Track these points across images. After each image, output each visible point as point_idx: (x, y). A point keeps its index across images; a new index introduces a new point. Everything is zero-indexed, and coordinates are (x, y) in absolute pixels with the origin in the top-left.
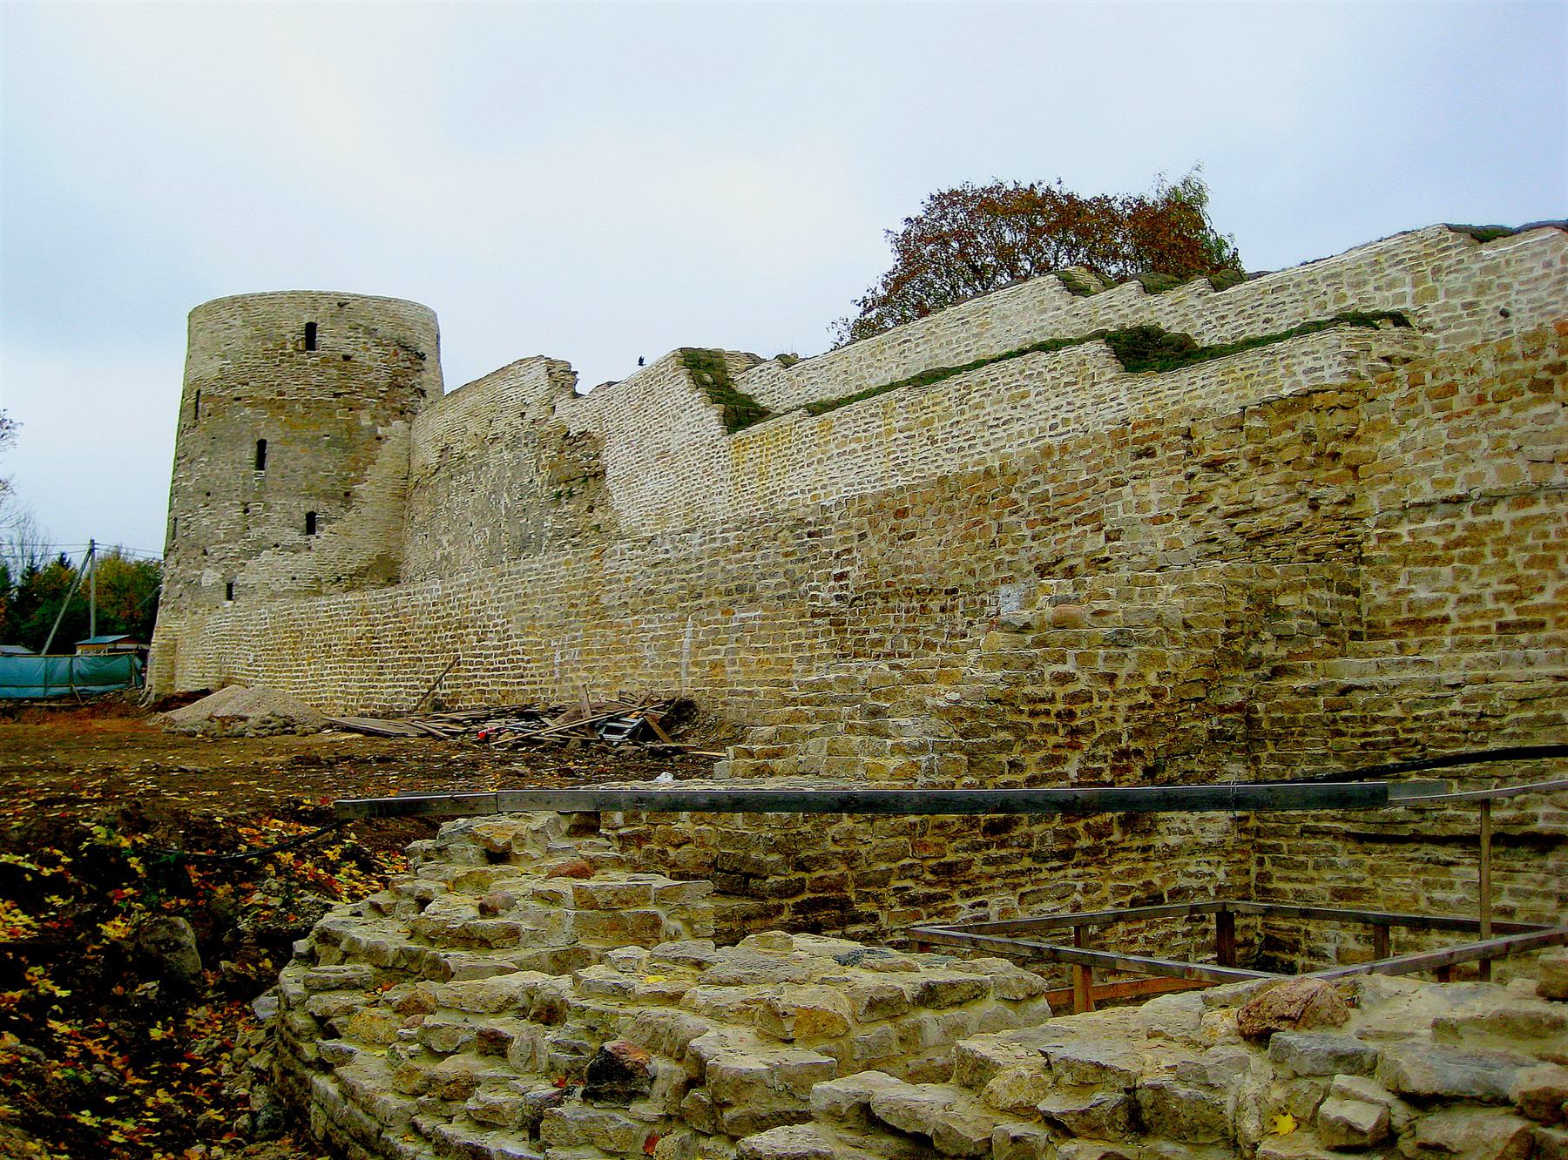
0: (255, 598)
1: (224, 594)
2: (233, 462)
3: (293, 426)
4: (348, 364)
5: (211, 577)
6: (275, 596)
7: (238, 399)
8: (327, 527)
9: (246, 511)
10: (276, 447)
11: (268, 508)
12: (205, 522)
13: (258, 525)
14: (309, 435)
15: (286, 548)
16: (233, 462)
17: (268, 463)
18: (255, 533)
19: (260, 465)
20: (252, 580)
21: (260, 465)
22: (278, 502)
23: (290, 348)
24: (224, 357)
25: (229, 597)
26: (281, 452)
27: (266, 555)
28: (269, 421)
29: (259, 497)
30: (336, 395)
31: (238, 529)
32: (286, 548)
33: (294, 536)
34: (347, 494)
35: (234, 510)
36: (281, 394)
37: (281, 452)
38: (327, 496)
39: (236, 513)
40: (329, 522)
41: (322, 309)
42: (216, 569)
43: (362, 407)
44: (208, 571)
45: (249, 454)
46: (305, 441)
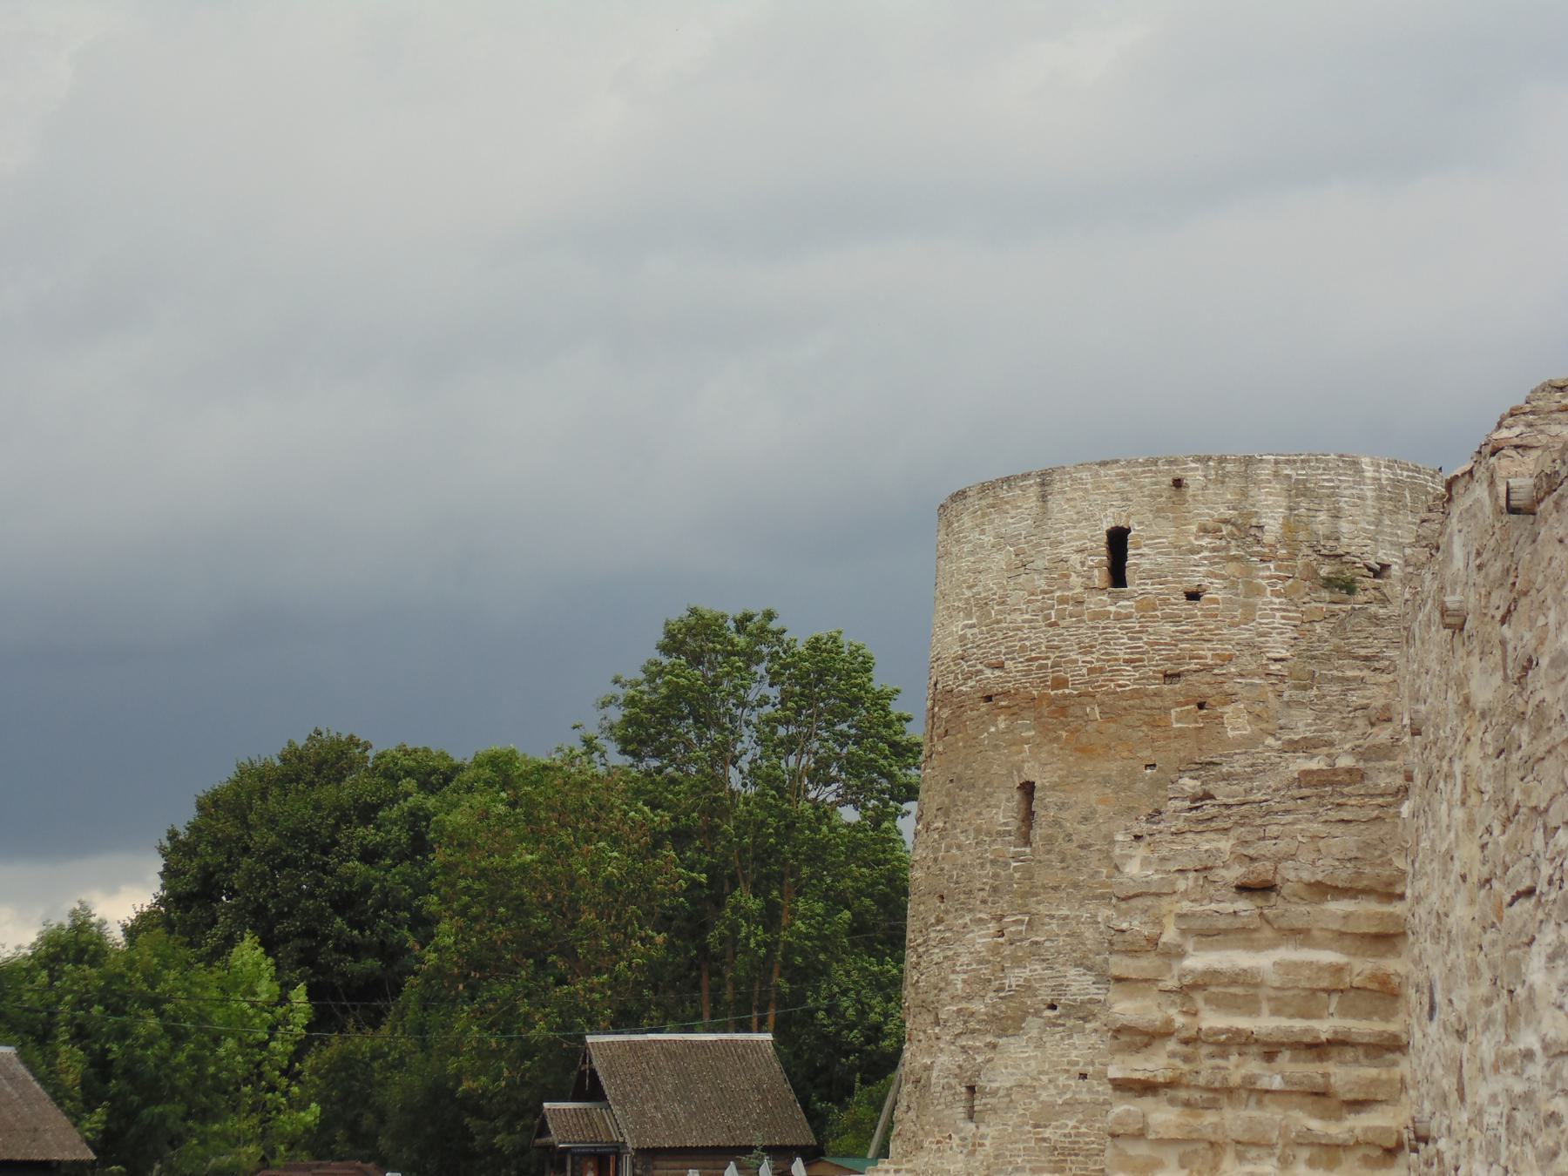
2: (978, 831)
4: (1197, 609)
7: (989, 699)
10: (1052, 798)
13: (1018, 962)
16: (978, 831)
17: (1037, 833)
18: (1015, 977)
36: (1060, 683)
43: (1229, 698)
45: (1004, 812)
46: (1106, 781)
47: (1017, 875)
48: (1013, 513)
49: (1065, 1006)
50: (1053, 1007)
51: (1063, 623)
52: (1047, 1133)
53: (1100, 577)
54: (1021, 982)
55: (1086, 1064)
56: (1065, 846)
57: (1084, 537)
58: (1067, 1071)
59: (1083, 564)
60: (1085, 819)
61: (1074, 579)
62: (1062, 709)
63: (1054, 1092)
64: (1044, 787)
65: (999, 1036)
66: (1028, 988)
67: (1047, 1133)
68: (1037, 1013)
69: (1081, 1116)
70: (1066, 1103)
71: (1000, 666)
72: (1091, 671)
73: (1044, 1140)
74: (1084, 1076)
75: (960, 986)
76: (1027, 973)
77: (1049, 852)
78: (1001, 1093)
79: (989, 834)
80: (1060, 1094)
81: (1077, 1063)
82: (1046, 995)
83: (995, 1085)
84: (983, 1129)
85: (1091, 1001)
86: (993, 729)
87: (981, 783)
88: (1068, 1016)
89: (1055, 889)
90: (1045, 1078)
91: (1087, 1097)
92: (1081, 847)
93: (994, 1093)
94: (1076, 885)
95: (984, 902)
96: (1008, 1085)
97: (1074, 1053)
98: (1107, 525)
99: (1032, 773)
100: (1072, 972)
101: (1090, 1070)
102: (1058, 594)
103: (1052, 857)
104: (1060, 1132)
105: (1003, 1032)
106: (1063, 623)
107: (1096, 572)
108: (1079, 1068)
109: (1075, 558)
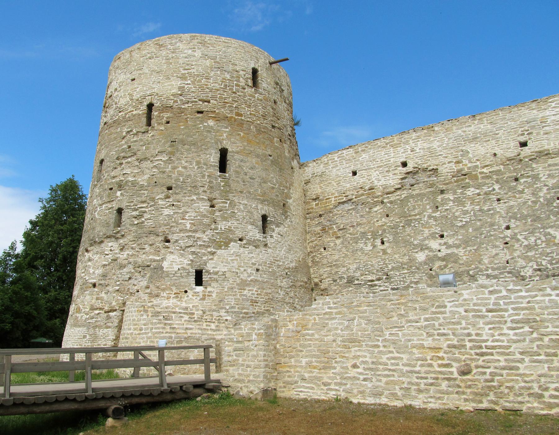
0: (227, 285)
1: (192, 279)
2: (198, 163)
3: (249, 142)
5: (175, 262)
6: (243, 284)
7: (201, 112)
8: (277, 230)
9: (212, 206)
11: (232, 204)
12: (166, 212)
13: (225, 219)
14: (260, 151)
15: (250, 242)
18: (222, 226)
19: (223, 167)
20: (221, 268)
21: (223, 167)
22: (242, 202)
23: (242, 83)
24: (183, 77)
25: (199, 281)
26: (242, 161)
27: (234, 247)
28: (230, 135)
29: (226, 193)
30: (273, 127)
31: (206, 221)
32: (250, 242)
33: (255, 233)
34: (284, 205)
35: (201, 204)
36: (238, 114)
37: (242, 161)
38: (272, 203)
39: (204, 207)
40: (277, 226)
41: (260, 61)
42: (182, 255)
44: (170, 257)
45: (214, 158)
46: (258, 156)
47: (222, 184)
48: (212, 48)
49: (248, 240)
50: (241, 240)
51: (238, 93)
52: (245, 292)
53: (250, 83)
54: (227, 227)
55: (259, 265)
56: (245, 177)
57: (244, 66)
58: (252, 267)
59: (245, 75)
60: (252, 168)
61: (241, 79)
62: (241, 124)
63: (246, 275)
64: (233, 152)
65: (217, 249)
66: (230, 230)
67: (245, 292)
68: (235, 241)
69: (258, 287)
70: (251, 281)
71: (209, 102)
72: (251, 114)
73: (244, 295)
74: (258, 270)
75: (188, 226)
76: (229, 224)
77: (237, 177)
78: (220, 273)
79: (205, 164)
80: (249, 276)
81: (255, 264)
82: (239, 234)
83: (216, 270)
84: (209, 289)
85: (257, 240)
86: (206, 124)
87: (199, 144)
88: (250, 244)
89: (241, 192)
90: (242, 269)
91: (260, 279)
92: (250, 178)
93: (216, 273)
94: (249, 193)
95: (205, 192)
96: (223, 270)
97: (254, 260)
98: (253, 66)
99: (226, 144)
100: (250, 227)
101: (260, 268)
102: (235, 82)
103: (239, 179)
104: (251, 292)
105: (220, 247)
106: (238, 93)
107: (249, 80)
108: (256, 266)
109: (242, 73)
